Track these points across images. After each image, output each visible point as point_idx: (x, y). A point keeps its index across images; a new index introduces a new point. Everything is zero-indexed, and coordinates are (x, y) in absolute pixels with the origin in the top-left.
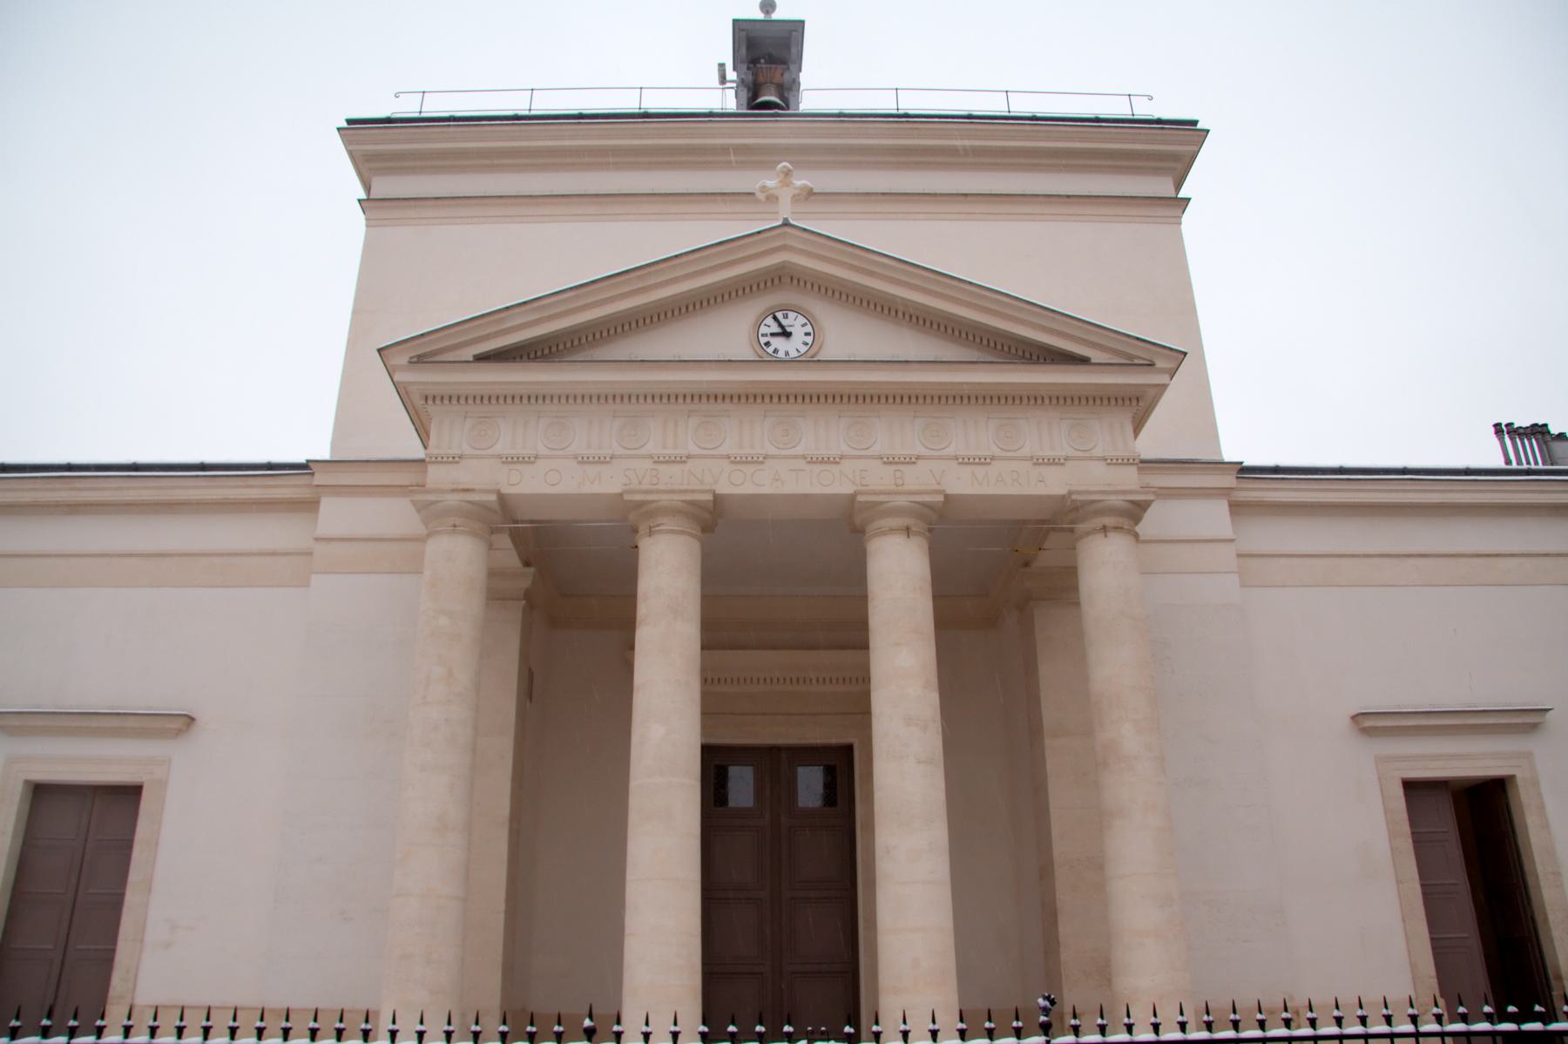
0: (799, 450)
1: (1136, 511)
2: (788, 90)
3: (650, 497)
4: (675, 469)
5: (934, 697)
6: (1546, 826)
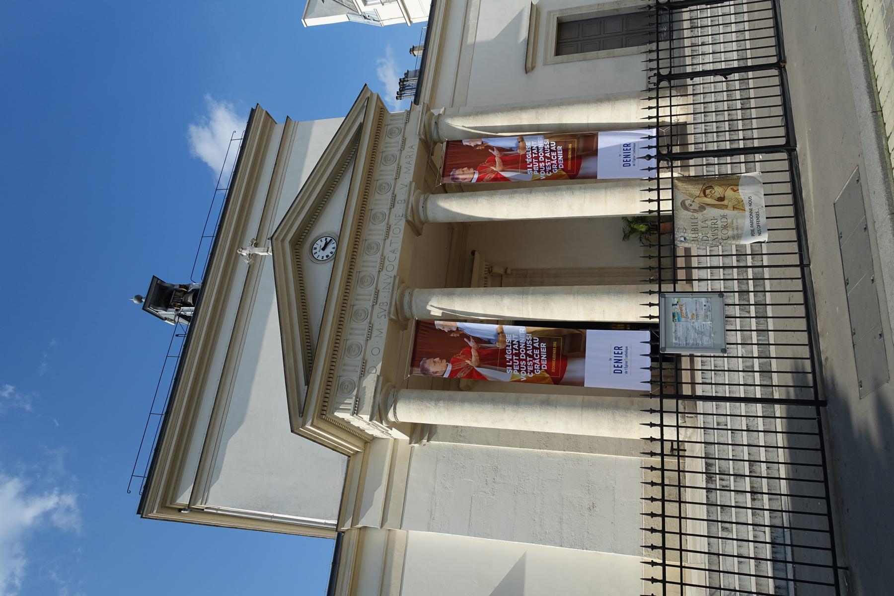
3: (394, 303)
4: (381, 295)
6: (579, 8)
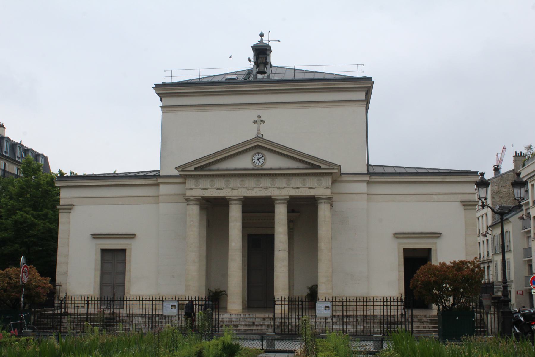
0: (260, 186)
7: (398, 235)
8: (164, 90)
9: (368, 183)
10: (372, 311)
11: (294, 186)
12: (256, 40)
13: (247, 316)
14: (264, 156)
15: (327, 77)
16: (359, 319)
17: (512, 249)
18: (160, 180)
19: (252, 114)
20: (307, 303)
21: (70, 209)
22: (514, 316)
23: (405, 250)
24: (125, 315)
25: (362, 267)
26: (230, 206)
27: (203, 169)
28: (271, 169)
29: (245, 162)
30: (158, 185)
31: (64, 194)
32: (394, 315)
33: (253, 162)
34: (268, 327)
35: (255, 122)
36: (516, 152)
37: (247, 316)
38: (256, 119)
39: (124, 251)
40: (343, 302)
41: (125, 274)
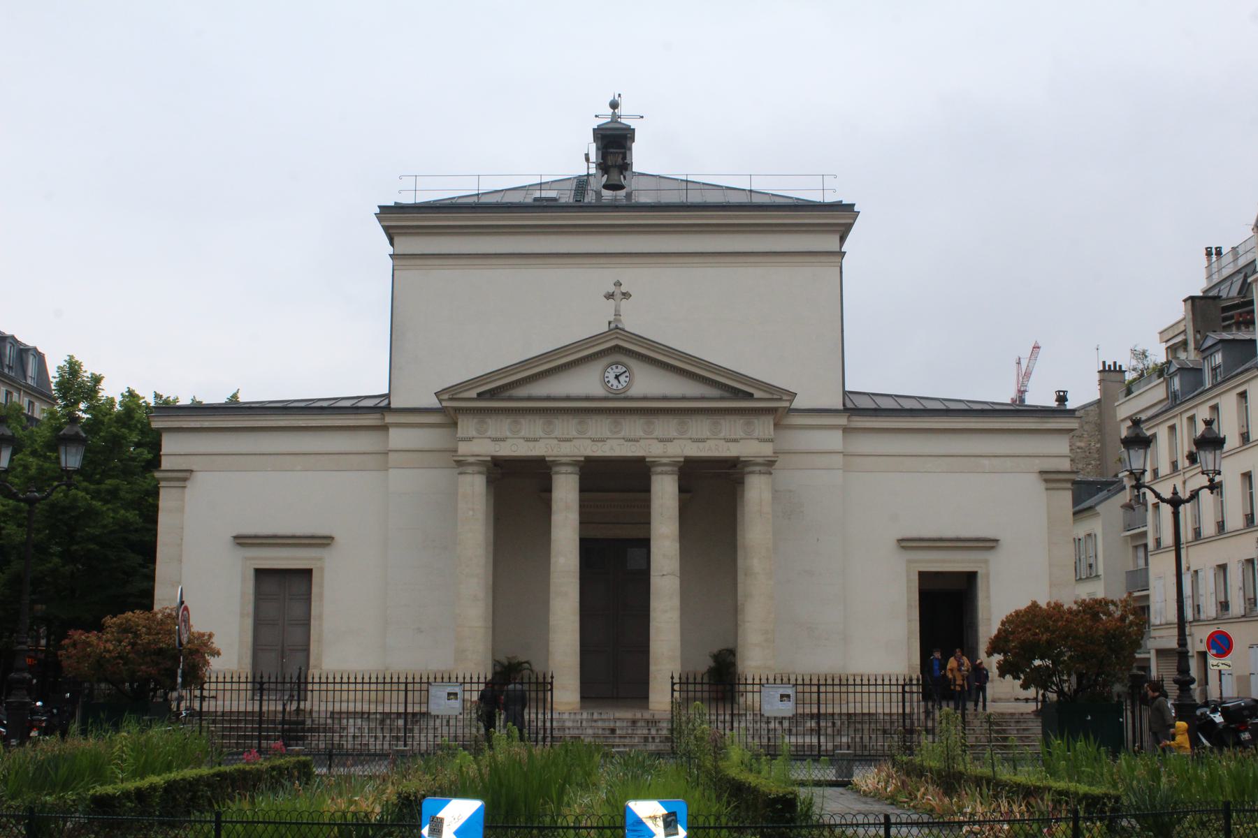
1: (771, 463)
2: (625, 167)
4: (568, 444)
5: (677, 545)
6: (988, 597)
7: (906, 544)
8: (399, 220)
9: (846, 430)
10: (851, 705)
11: (694, 436)
12: (605, 115)
13: (596, 716)
14: (628, 369)
15: (757, 199)
16: (838, 723)
17: (1101, 572)
18: (389, 419)
19: (603, 277)
20: (706, 687)
21: (185, 480)
22: (1198, 712)
23: (922, 575)
24: (323, 715)
25: (828, 612)
26: (555, 477)
27: (497, 395)
28: (645, 399)
29: (586, 383)
30: (385, 428)
31: (169, 445)
32: (911, 714)
33: (606, 383)
34: (646, 739)
35: (610, 296)
36: (1104, 363)
37: (596, 716)
38: (612, 289)
39: (307, 573)
40: (819, 685)
41: (309, 625)
